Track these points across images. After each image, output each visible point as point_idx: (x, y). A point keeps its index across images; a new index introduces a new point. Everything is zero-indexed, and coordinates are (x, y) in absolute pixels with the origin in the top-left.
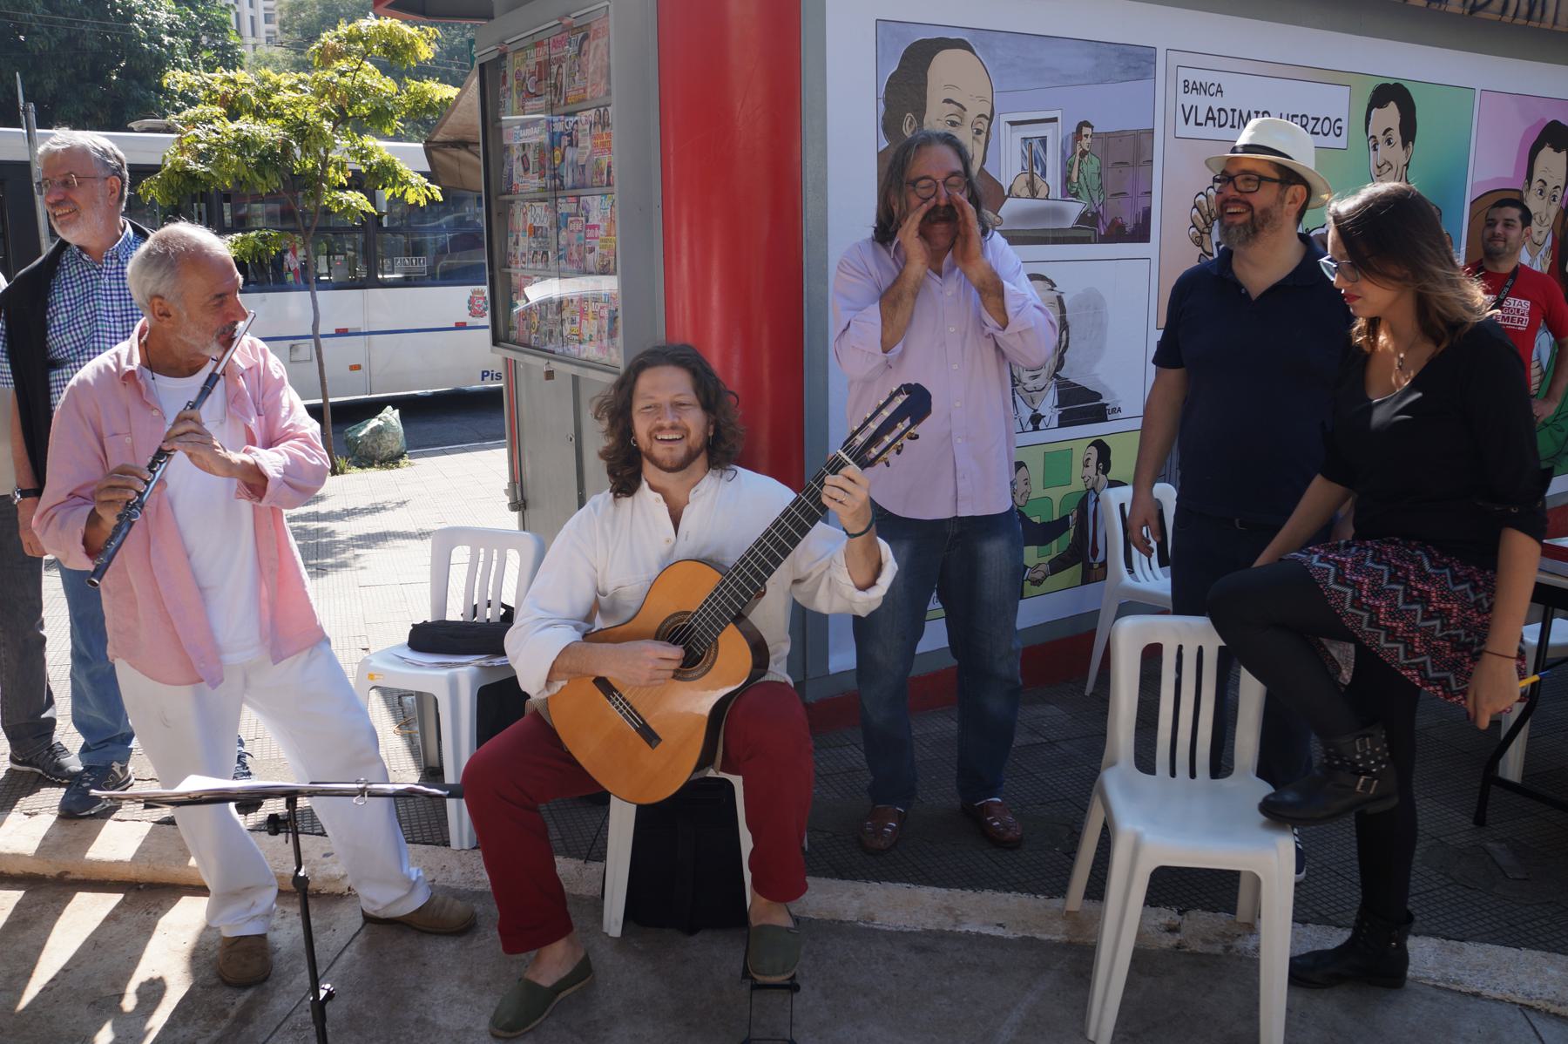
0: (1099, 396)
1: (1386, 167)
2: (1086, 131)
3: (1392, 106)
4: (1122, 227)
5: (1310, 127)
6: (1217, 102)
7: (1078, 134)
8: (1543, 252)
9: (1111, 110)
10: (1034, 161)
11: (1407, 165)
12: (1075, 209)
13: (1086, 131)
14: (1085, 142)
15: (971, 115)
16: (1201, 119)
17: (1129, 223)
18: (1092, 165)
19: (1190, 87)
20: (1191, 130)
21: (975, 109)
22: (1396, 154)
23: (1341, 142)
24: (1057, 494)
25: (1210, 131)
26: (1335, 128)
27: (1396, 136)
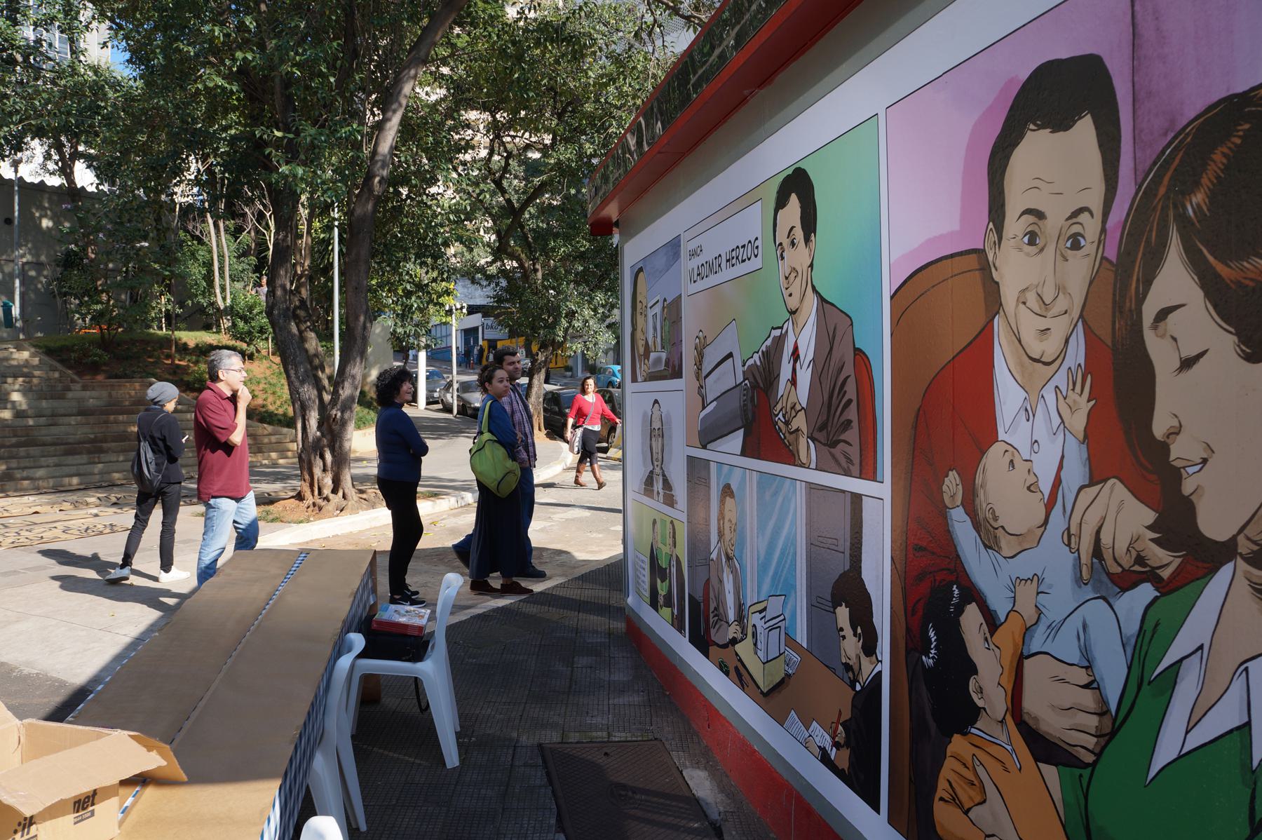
1: (793, 275)
8: (1061, 379)
11: (811, 266)
19: (693, 254)
27: (799, 234)
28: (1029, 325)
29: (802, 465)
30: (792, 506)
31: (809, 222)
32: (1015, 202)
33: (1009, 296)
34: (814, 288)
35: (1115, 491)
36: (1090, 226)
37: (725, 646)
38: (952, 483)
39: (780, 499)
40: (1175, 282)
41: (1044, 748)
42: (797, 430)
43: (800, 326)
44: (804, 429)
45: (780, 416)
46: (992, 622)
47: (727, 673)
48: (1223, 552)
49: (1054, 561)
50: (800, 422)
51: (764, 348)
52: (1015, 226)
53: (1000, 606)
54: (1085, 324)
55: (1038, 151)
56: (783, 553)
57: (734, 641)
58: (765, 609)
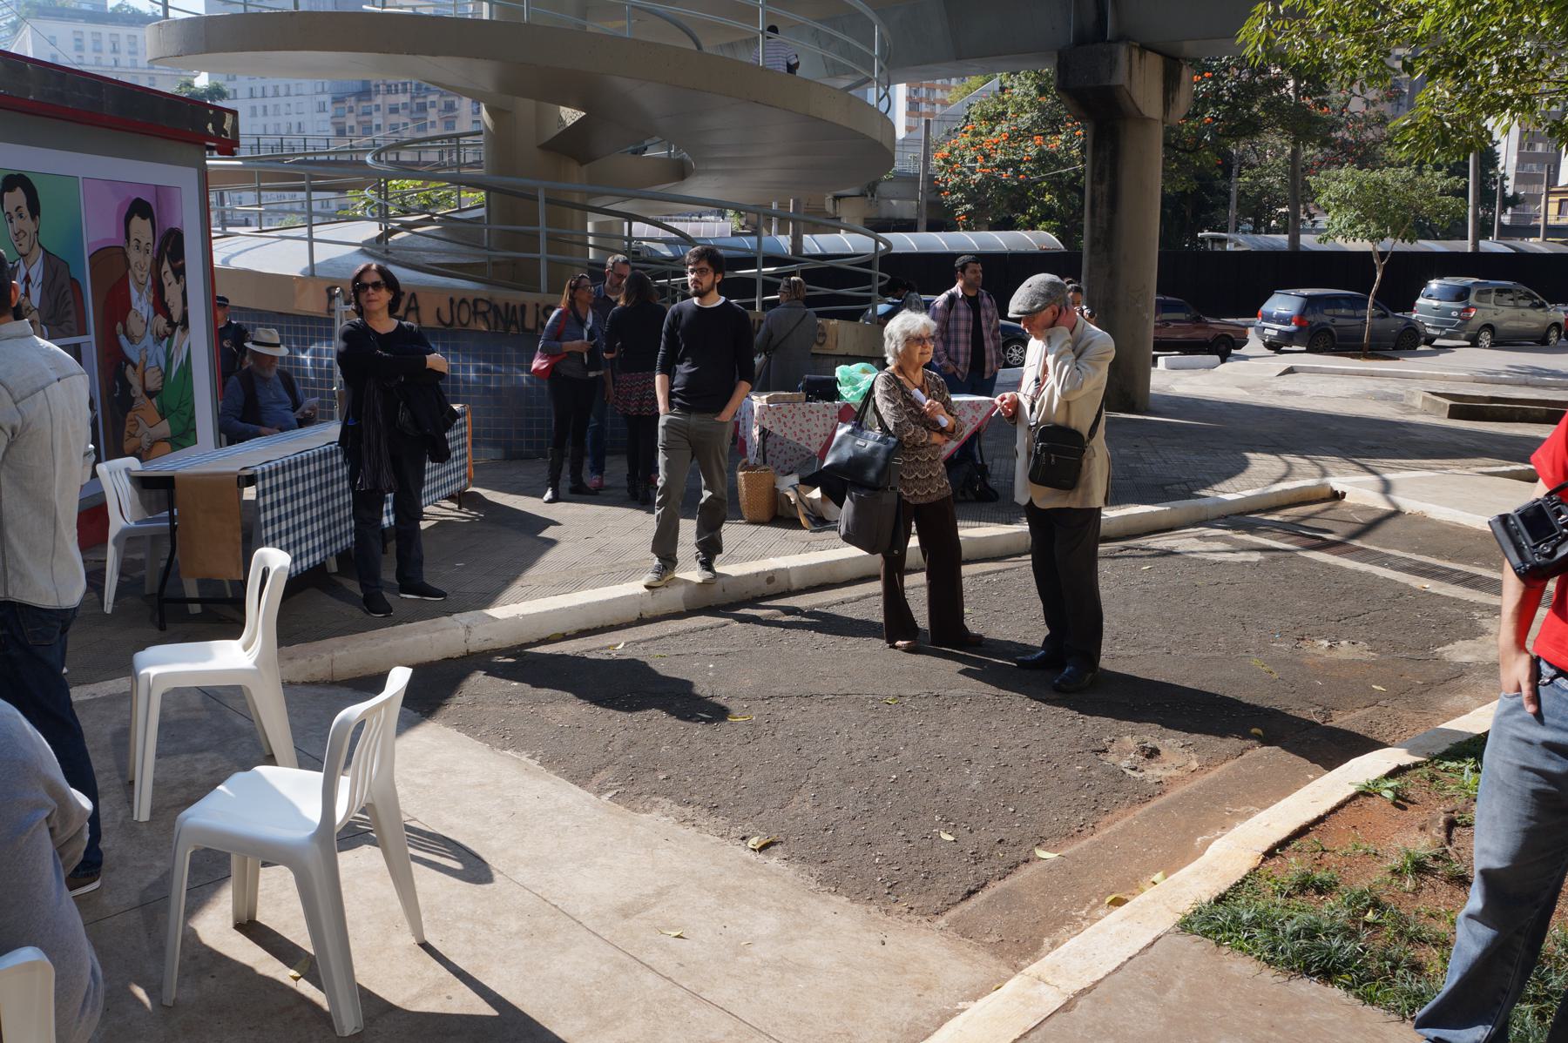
3: (19, 189)
22: (28, 224)
28: (138, 273)
31: (34, 208)
32: (133, 236)
33: (132, 264)
35: (160, 316)
38: (119, 326)
40: (166, 267)
41: (151, 394)
46: (135, 367)
49: (149, 340)
52: (133, 243)
53: (136, 360)
55: (137, 222)
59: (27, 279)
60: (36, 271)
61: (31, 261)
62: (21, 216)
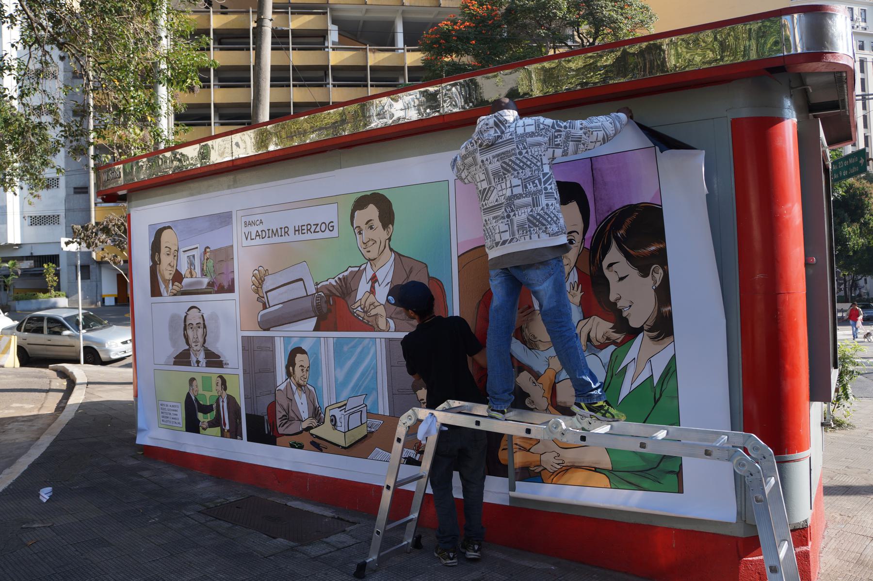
0: (219, 357)
2: (208, 250)
4: (223, 287)
5: (312, 230)
6: (259, 228)
7: (205, 252)
9: (216, 240)
10: (191, 264)
12: (206, 281)
13: (208, 250)
14: (208, 254)
15: (172, 251)
16: (253, 237)
17: (226, 285)
18: (211, 263)
19: (247, 224)
20: (250, 242)
21: (174, 248)
22: (380, 234)
23: (335, 233)
24: (208, 394)
25: (258, 241)
26: (330, 227)
27: (377, 223)
29: (381, 331)
30: (372, 351)
31: (387, 217)
34: (391, 250)
36: (578, 238)
37: (301, 432)
39: (359, 349)
42: (377, 315)
43: (378, 266)
44: (384, 314)
45: (359, 309)
47: (301, 447)
48: (634, 333)
50: (381, 310)
51: (341, 276)
54: (578, 270)
56: (363, 374)
57: (308, 429)
58: (345, 405)
59: (374, 279)
60: (386, 273)
61: (379, 264)
62: (371, 228)
